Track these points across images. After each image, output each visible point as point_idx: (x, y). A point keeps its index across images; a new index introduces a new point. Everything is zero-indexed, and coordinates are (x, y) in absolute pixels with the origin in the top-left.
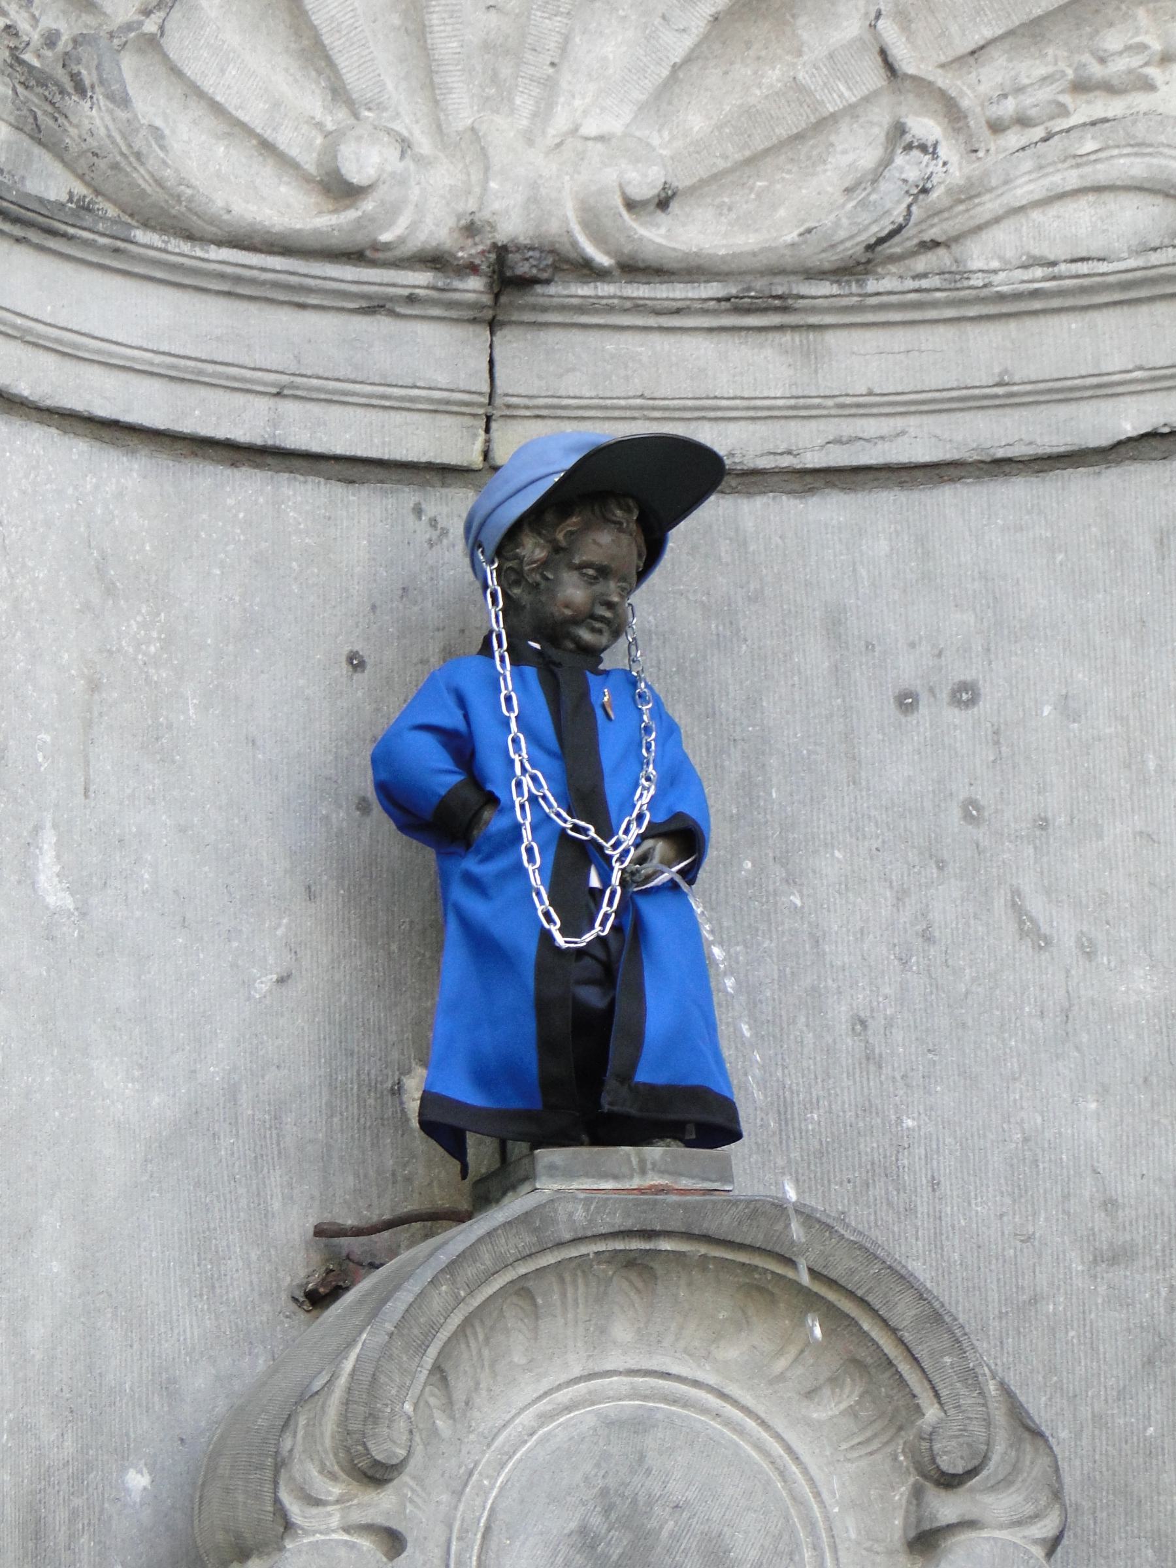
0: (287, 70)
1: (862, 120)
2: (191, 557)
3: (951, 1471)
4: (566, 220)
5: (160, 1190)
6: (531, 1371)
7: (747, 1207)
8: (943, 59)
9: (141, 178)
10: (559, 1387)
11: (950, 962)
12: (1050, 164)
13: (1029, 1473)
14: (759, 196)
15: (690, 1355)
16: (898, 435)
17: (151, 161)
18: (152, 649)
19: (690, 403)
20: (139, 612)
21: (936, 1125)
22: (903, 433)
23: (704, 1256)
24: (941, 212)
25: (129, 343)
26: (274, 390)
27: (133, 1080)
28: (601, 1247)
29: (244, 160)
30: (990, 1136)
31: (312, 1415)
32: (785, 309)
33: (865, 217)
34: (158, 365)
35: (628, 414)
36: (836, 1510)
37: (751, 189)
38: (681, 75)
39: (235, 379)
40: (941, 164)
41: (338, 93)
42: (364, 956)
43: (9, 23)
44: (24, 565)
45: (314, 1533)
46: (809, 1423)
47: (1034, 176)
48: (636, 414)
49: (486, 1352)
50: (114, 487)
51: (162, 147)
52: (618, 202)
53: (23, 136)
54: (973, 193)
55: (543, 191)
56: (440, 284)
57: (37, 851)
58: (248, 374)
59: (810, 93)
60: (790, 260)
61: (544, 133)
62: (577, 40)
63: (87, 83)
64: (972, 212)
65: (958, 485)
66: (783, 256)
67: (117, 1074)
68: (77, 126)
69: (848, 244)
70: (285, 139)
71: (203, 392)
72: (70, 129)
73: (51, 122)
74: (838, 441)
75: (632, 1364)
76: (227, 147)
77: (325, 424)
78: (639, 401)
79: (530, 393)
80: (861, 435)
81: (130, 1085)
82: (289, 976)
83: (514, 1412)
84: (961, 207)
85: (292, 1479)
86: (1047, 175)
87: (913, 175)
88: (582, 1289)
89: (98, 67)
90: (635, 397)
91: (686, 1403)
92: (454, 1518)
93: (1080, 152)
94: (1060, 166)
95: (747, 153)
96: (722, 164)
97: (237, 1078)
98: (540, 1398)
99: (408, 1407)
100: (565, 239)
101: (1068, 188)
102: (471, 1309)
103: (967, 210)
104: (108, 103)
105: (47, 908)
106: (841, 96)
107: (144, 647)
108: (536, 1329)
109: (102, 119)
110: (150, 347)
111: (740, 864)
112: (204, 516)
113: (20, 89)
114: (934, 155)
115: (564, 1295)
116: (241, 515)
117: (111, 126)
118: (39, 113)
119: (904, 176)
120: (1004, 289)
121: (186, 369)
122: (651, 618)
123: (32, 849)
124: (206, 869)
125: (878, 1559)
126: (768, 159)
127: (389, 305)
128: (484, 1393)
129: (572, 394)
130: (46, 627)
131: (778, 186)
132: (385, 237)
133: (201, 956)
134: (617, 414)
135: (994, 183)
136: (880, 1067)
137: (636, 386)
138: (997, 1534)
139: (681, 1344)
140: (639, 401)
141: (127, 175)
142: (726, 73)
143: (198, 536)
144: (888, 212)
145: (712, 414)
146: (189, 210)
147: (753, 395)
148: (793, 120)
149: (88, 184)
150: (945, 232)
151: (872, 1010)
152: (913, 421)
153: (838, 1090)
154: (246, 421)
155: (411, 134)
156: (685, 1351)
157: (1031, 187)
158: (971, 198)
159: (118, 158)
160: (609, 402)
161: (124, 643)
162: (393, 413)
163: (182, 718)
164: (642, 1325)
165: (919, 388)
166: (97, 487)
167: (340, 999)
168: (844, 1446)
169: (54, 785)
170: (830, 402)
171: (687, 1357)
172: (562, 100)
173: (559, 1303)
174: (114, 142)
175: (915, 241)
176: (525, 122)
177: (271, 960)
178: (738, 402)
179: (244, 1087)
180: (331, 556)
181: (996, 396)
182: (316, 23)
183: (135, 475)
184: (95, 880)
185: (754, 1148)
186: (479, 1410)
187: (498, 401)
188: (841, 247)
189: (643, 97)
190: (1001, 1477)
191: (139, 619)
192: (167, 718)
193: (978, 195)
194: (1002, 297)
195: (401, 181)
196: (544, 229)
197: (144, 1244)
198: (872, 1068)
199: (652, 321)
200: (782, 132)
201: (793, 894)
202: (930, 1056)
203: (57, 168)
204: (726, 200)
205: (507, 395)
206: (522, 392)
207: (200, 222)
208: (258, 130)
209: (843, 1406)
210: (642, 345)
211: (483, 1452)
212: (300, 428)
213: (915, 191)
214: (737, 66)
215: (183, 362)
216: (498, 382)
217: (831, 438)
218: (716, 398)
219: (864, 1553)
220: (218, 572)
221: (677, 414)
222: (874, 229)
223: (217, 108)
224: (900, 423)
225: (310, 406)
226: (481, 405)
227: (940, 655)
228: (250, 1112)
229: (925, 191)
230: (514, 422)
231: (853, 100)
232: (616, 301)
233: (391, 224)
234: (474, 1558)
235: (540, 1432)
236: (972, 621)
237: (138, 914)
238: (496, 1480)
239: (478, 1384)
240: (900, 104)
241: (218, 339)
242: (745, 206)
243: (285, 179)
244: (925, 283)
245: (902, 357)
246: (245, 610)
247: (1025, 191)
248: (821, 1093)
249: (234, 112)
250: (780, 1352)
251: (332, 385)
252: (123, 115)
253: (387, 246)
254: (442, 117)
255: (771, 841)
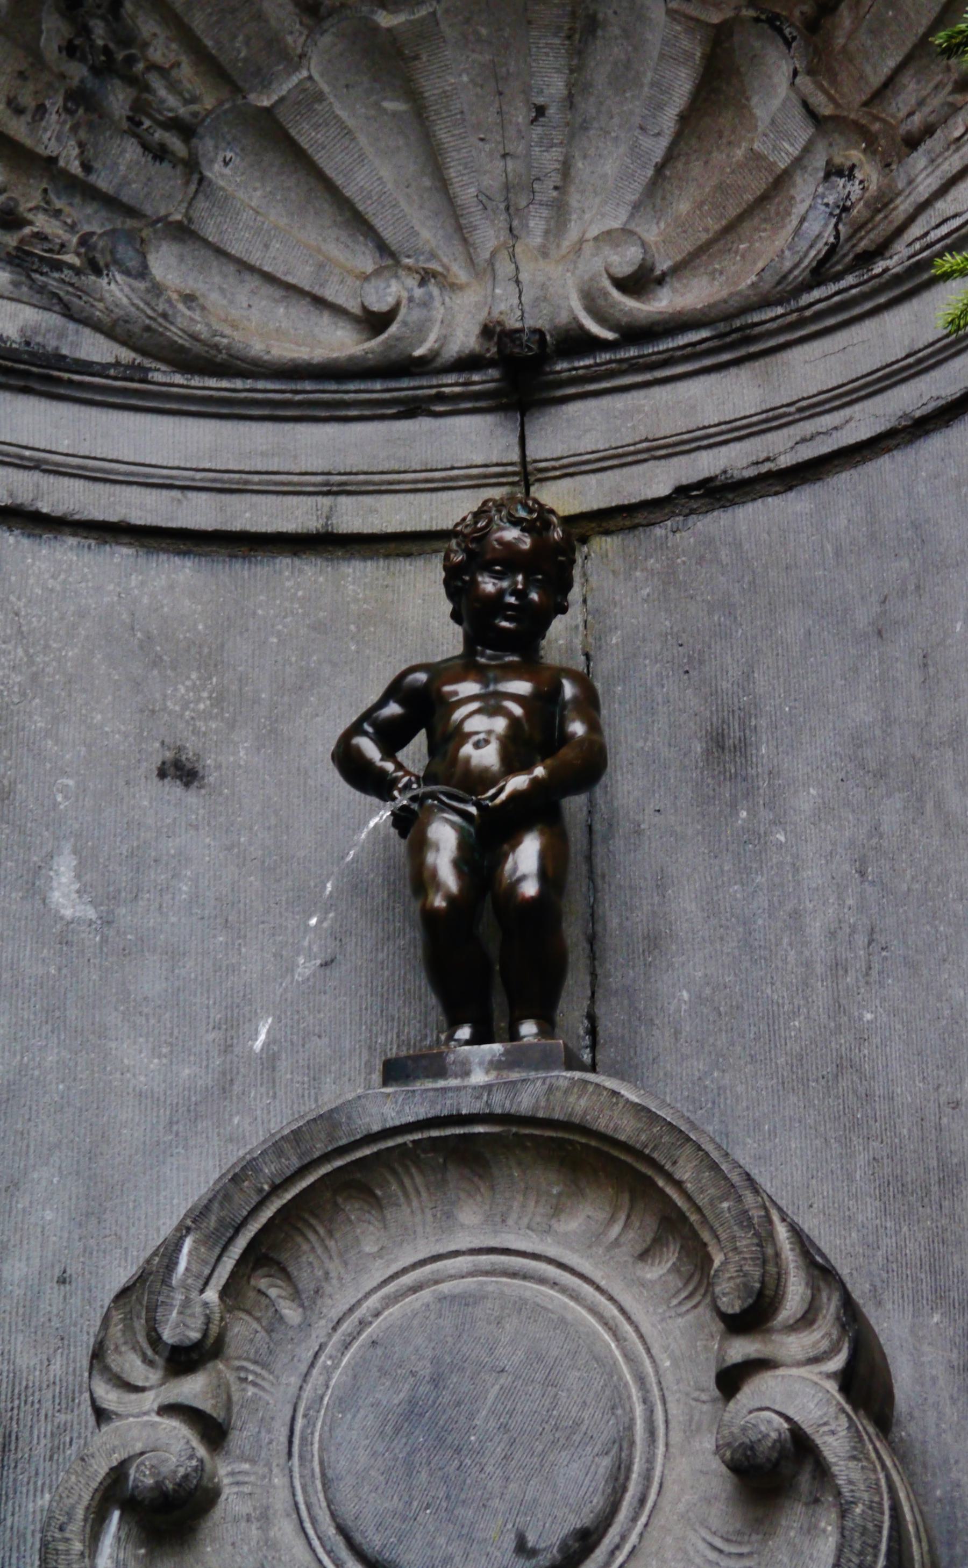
0: (337, 239)
1: (810, 169)
2: (247, 630)
3: (730, 1311)
4: (571, 310)
5: (186, 1147)
6: (381, 1257)
7: (544, 1083)
8: (864, 98)
9: (174, 333)
10: (405, 1271)
11: (896, 867)
12: (938, 156)
13: (828, 1310)
14: (743, 257)
15: (533, 1230)
16: (847, 422)
17: (179, 320)
18: (202, 706)
19: (685, 437)
20: (188, 678)
21: (889, 1015)
22: (851, 419)
23: (516, 1134)
24: (866, 223)
25: (165, 464)
26: (325, 489)
27: (159, 1057)
28: (417, 1136)
29: (303, 316)
30: (928, 1016)
31: (128, 1309)
32: (748, 340)
33: (803, 245)
34: (201, 480)
35: (640, 457)
36: (668, 1364)
37: (736, 252)
38: (668, 173)
39: (283, 484)
40: (857, 182)
41: (383, 248)
42: (407, 937)
43: (36, 230)
44: (47, 646)
45: (128, 1416)
46: (643, 1284)
47: (929, 170)
48: (645, 456)
49: (331, 1244)
50: (163, 582)
51: (189, 308)
52: (607, 284)
53: (55, 316)
54: (886, 200)
55: (551, 290)
56: (461, 380)
57: (52, 873)
58: (295, 479)
59: (765, 158)
60: (755, 299)
61: (558, 246)
62: (580, 165)
63: (102, 263)
64: (890, 218)
65: (895, 452)
66: (748, 296)
67: (141, 1052)
68: (101, 300)
69: (796, 273)
70: (330, 293)
71: (255, 498)
72: (96, 303)
73: (75, 300)
74: (804, 440)
75: (476, 1244)
76: (287, 307)
77: (377, 511)
78: (645, 445)
79: (555, 456)
80: (820, 430)
81: (156, 1061)
82: (332, 961)
83: (360, 1296)
84: (881, 216)
85: (106, 1369)
86: (939, 166)
87: (831, 199)
88: (419, 1180)
89: (113, 252)
90: (641, 442)
91: (525, 1276)
92: (299, 1397)
93: (957, 134)
94: (947, 154)
95: (724, 222)
96: (704, 237)
97: (276, 1048)
98: (385, 1282)
99: (212, 1295)
100: (574, 325)
101: (954, 171)
102: (285, 1201)
103: (886, 217)
104: (124, 277)
105: (62, 918)
106: (787, 153)
107: (192, 705)
108: (383, 1220)
109: (122, 290)
110: (188, 465)
111: (737, 814)
112: (262, 598)
113: (36, 276)
114: (851, 177)
115: (402, 1185)
116: (300, 593)
117: (133, 296)
118: (62, 294)
119: (826, 200)
120: (898, 269)
121: (231, 481)
122: (667, 623)
123: (43, 871)
124: (252, 878)
125: (705, 1407)
126: (745, 224)
127: (424, 406)
128: (335, 1282)
129: (589, 450)
130: (74, 695)
131: (757, 245)
132: (418, 353)
133: (243, 950)
134: (630, 459)
135: (900, 186)
136: (846, 971)
137: (642, 432)
138: (794, 1371)
139: (526, 1220)
140: (645, 445)
141: (162, 334)
142: (706, 162)
143: (254, 613)
144: (819, 236)
145: (705, 442)
146: (231, 356)
147: (732, 418)
148: (757, 184)
149: (135, 349)
150: (872, 241)
151: (840, 922)
152: (857, 407)
153: (814, 997)
154: (298, 516)
155: (448, 270)
156: (529, 1227)
157: (929, 180)
158: (886, 205)
159: (147, 321)
160: (620, 451)
161: (169, 704)
162: (440, 494)
163: (232, 759)
164: (487, 1207)
165: (854, 377)
166: (143, 583)
167: (382, 975)
168: (675, 1302)
169: (76, 818)
170: (792, 409)
171: (530, 1233)
172: (574, 217)
173: (400, 1193)
174: (138, 308)
175: (851, 256)
176: (539, 240)
177: (315, 949)
178: (723, 427)
179: (284, 1056)
180: (388, 616)
181: (910, 366)
182: (348, 194)
183: (187, 571)
184: (123, 894)
185: (749, 1059)
186: (330, 1296)
187: (530, 468)
188: (791, 277)
189: (634, 198)
190: (799, 1316)
191: (188, 683)
192: (215, 760)
193: (892, 201)
194: (898, 279)
195: (426, 304)
196: (557, 321)
197: (163, 1193)
198: (841, 972)
199: (648, 377)
200: (749, 197)
201: (778, 832)
202: (884, 953)
203: (100, 338)
204: (717, 266)
205: (535, 461)
206: (549, 456)
207: (245, 365)
208: (307, 288)
209: (669, 1264)
210: (645, 397)
211: (330, 1336)
212: (353, 516)
213: (837, 211)
214: (715, 154)
215: (226, 476)
216: (528, 453)
217: (798, 438)
218: (705, 428)
219: (694, 1403)
220: (275, 640)
221: (678, 449)
222: (813, 253)
223: (269, 278)
224: (847, 412)
225: (361, 498)
226: (514, 474)
227: (884, 602)
228: (289, 1076)
229: (845, 209)
230: (549, 483)
231: (796, 153)
232: (614, 365)
233: (422, 342)
234: (317, 1435)
235: (386, 1313)
236: (907, 565)
237: (173, 919)
238: (341, 1360)
239: (327, 1273)
240: (831, 145)
241: (262, 454)
242: (733, 268)
243: (341, 324)
244: (843, 284)
245: (840, 355)
246: (301, 668)
247: (926, 185)
248: (802, 1002)
249: (283, 278)
250: (612, 1220)
251: (377, 478)
252: (141, 285)
253: (422, 360)
254: (472, 251)
255: (761, 791)
